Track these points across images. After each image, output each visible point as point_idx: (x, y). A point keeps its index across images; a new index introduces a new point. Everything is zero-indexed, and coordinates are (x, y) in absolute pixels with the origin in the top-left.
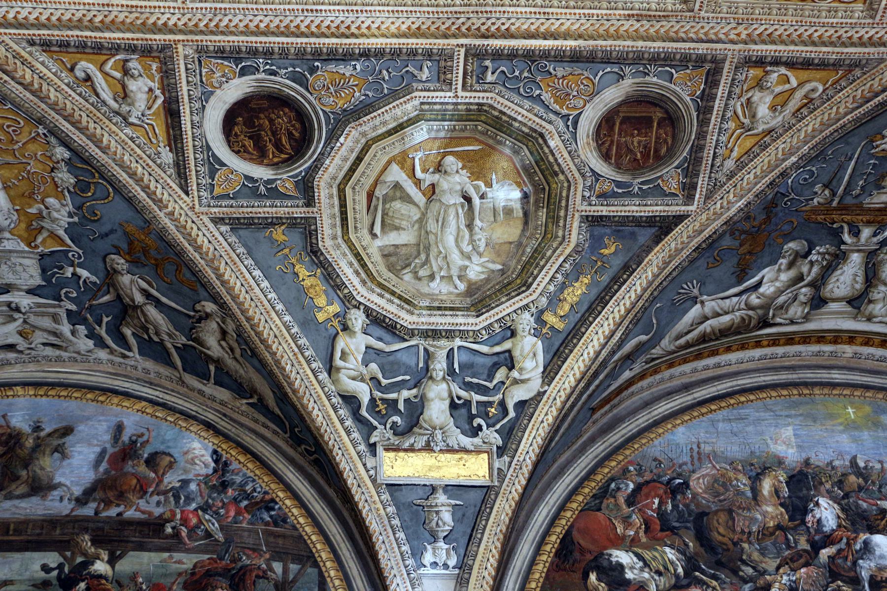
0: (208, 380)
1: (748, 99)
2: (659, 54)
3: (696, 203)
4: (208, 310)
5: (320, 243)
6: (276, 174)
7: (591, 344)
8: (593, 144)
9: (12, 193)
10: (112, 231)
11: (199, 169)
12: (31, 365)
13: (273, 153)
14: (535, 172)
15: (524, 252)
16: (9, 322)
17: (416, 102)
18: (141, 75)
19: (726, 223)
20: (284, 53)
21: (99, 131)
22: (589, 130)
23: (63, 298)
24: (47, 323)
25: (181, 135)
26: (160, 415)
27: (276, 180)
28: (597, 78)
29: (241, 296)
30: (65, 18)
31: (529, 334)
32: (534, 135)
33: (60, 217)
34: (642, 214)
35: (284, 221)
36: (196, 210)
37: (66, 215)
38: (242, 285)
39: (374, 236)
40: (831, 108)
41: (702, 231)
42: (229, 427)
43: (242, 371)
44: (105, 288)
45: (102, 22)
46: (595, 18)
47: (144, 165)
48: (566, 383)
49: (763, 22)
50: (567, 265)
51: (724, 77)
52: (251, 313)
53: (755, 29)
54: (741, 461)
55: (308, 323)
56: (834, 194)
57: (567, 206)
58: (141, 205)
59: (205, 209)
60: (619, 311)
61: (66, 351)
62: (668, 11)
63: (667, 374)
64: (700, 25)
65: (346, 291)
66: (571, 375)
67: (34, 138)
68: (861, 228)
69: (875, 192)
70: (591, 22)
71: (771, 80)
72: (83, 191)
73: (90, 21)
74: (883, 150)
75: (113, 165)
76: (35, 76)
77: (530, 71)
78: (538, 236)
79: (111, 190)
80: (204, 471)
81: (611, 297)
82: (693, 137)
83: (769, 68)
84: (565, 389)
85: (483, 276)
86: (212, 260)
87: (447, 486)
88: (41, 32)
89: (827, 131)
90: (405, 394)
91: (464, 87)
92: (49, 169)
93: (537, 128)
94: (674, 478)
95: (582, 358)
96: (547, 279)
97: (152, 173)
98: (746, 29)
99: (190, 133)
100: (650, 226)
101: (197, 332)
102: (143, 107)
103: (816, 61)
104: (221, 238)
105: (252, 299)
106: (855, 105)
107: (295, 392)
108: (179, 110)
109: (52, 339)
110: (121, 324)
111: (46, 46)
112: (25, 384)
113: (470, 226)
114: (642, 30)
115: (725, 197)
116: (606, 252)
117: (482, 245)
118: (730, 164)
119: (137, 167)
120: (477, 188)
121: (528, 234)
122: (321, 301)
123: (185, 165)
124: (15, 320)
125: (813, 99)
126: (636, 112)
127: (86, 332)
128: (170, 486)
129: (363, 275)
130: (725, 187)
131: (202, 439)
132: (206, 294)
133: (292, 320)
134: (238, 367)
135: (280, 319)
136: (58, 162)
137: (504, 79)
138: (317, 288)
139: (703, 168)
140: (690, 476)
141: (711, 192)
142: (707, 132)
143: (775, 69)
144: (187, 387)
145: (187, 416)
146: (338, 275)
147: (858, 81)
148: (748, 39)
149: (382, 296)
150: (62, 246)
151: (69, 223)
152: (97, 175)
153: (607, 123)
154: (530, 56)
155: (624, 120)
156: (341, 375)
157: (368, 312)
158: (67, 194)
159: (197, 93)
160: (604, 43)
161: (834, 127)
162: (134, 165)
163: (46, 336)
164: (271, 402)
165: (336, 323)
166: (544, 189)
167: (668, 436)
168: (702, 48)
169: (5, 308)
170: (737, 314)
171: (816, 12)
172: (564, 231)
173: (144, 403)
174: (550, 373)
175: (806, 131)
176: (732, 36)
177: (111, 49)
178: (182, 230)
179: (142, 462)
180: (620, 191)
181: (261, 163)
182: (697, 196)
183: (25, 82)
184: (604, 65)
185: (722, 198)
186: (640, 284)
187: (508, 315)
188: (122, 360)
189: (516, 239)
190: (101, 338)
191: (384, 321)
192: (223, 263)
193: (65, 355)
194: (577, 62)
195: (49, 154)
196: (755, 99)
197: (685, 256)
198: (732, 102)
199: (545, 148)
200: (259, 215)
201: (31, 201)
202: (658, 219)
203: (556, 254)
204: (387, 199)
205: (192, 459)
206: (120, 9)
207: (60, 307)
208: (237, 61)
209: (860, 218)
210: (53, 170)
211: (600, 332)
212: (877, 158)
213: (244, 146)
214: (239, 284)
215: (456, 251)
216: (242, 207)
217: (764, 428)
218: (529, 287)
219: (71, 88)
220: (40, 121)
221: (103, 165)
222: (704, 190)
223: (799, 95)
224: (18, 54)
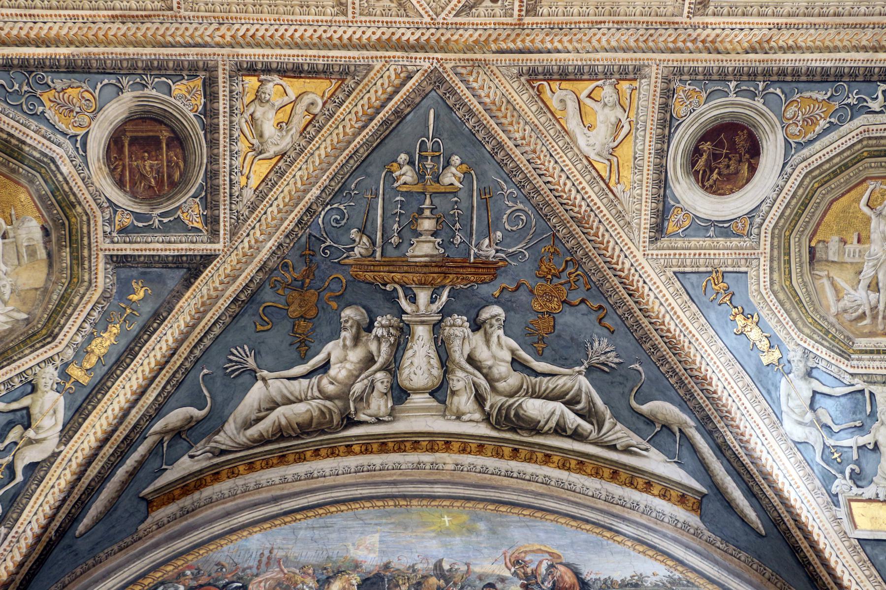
1: (251, 115)
2: (151, 61)
3: (221, 240)
7: (117, 399)
8: (105, 170)
14: (52, 204)
15: (50, 299)
19: (260, 269)
22: (99, 152)
28: (97, 91)
31: (52, 389)
32: (45, 160)
34: (168, 253)
40: (337, 127)
41: (236, 278)
46: (81, 20)
48: (86, 442)
49: (243, 21)
50: (95, 314)
51: (221, 89)
53: (238, 30)
54: (313, 566)
56: (374, 243)
57: (90, 244)
60: (149, 364)
62: (149, 10)
63: (252, 479)
64: (184, 26)
66: (91, 434)
68: (415, 291)
69: (414, 240)
70: (78, 25)
71: (268, 91)
74: (405, 183)
77: (28, 84)
78: (63, 281)
81: (141, 348)
82: (205, 161)
83: (262, 77)
84: (83, 449)
85: (7, 327)
89: (341, 158)
93: (47, 151)
94: (234, 582)
95: (105, 415)
96: (75, 329)
98: (228, 30)
100: (177, 267)
103: (306, 67)
106: (360, 124)
114: (129, 33)
115: (252, 233)
116: (134, 297)
118: (249, 195)
121: (53, 279)
125: (315, 115)
126: (142, 132)
130: (249, 222)
139: (222, 198)
140: (251, 580)
141: (235, 227)
142: (218, 155)
143: (269, 77)
147: (354, 94)
148: (233, 41)
153: (115, 142)
154: (25, 66)
155: (134, 141)
160: (96, 50)
161: (347, 152)
166: (63, 224)
167: (240, 542)
168: (192, 54)
170: (314, 403)
171: (289, 7)
172: (90, 274)
174: (68, 432)
175: (319, 155)
176: (218, 39)
180: (140, 225)
182: (222, 232)
184: (102, 76)
185: (248, 235)
186: (172, 334)
187: (31, 368)
189: (42, 285)
194: (74, 72)
196: (258, 115)
197: (223, 308)
198: (236, 119)
199: (59, 176)
202: (184, 259)
203: (84, 301)
209: (410, 276)
211: (127, 387)
212: (403, 194)
217: (348, 535)
218: (55, 338)
222: (228, 224)
223: (300, 108)
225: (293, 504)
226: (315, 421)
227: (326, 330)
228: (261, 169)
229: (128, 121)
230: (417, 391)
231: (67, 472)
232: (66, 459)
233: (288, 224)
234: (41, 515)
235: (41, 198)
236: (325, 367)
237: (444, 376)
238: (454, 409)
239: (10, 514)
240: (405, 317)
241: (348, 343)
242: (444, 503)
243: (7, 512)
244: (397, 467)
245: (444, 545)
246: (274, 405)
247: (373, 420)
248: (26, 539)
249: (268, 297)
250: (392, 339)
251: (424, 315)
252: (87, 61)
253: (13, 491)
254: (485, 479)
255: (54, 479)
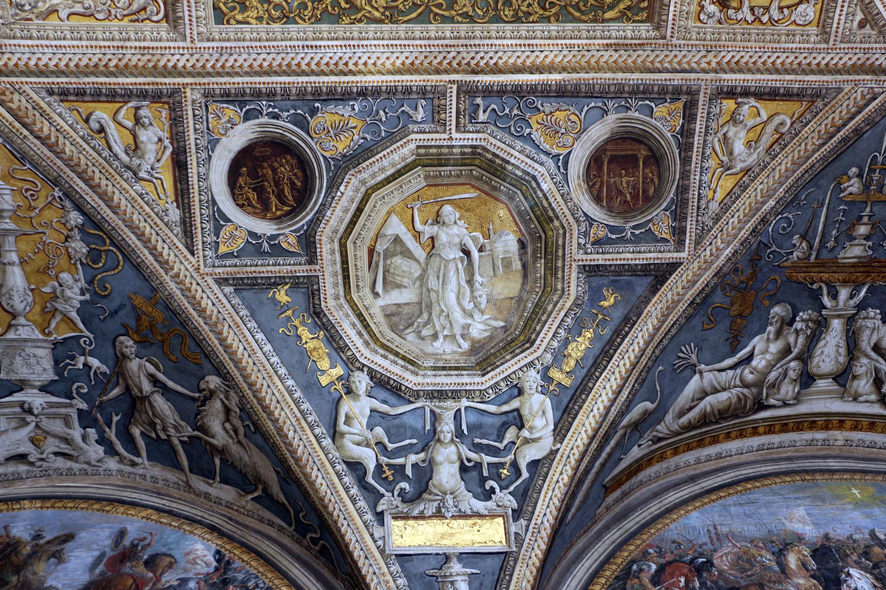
0: (214, 479)
1: (724, 135)
2: (638, 86)
3: (687, 249)
4: (212, 386)
5: (323, 304)
6: (279, 229)
7: (600, 399)
8: (584, 186)
9: (28, 268)
10: (122, 307)
11: (204, 226)
12: (42, 480)
13: (276, 205)
14: (531, 218)
15: (525, 307)
16: (21, 426)
17: (412, 146)
18: (151, 124)
19: (716, 274)
20: (286, 93)
21: (110, 188)
22: (579, 170)
23: (75, 395)
24: (57, 426)
25: (188, 189)
26: (165, 521)
27: (279, 235)
28: (583, 114)
29: (244, 361)
30: (82, 63)
31: (537, 391)
32: (527, 178)
33: (72, 295)
34: (637, 262)
35: (287, 280)
36: (201, 271)
37: (79, 292)
38: (245, 349)
39: (376, 295)
40: (800, 145)
41: (695, 282)
42: (234, 530)
43: (246, 458)
44: (114, 379)
45: (116, 66)
46: (576, 48)
47: (152, 224)
48: (579, 440)
49: (730, 49)
50: (569, 320)
51: (700, 111)
52: (253, 378)
53: (724, 57)
54: (760, 539)
55: (311, 387)
56: (811, 247)
57: (564, 255)
58: (148, 271)
59: (209, 270)
60: (624, 365)
61: (77, 462)
62: (642, 39)
63: (673, 462)
64: (673, 53)
65: (349, 353)
66: (583, 432)
67: (50, 203)
68: (838, 288)
69: (847, 244)
70: (573, 53)
71: (743, 113)
72: (95, 262)
73: (106, 66)
74: (851, 194)
75: (123, 227)
76: (53, 129)
77: (519, 108)
78: (537, 290)
79: (121, 258)
80: (205, 570)
81: (615, 351)
82: (678, 177)
83: (740, 100)
84: (578, 447)
85: (486, 334)
86: (215, 324)
87: (461, 553)
88: (60, 80)
89: (798, 172)
90: (413, 458)
91: (458, 130)
92: (63, 238)
93: (530, 170)
94: (697, 558)
95: (592, 414)
96: (550, 335)
97: (159, 232)
98: (715, 57)
99: (196, 187)
100: (646, 275)
101: (202, 418)
102: (153, 159)
103: (782, 91)
104: (224, 301)
105: (254, 364)
106: (821, 141)
107: (297, 460)
108: (186, 162)
109: (64, 448)
110: (130, 423)
111: (64, 94)
112: (32, 498)
113: (470, 282)
114: (620, 60)
115: (714, 242)
116: (605, 304)
117: (483, 301)
118: (714, 207)
119: (145, 227)
120: (474, 239)
121: (528, 288)
122: (324, 364)
123: (191, 222)
124: (28, 424)
125: (782, 134)
126: (622, 150)
127: (96, 437)
128: (168, 584)
129: (366, 336)
130: (713, 232)
131: (205, 541)
132: (210, 366)
133: (294, 384)
134: (242, 452)
135: (283, 383)
136: (71, 230)
137: (496, 118)
138: (320, 351)
139: (690, 211)
140: (712, 555)
141: (700, 237)
142: (689, 171)
143: (746, 100)
144: (194, 492)
145: (192, 521)
146: (341, 337)
147: (821, 114)
148: (718, 68)
149: (386, 357)
150: (74, 331)
151: (81, 302)
152: (108, 241)
153: (595, 161)
154: (518, 91)
155: (612, 160)
156: (345, 440)
157: (372, 374)
158: (79, 266)
159: (203, 142)
160: (586, 76)
161: (804, 167)
162: (142, 224)
163: (57, 444)
164: (275, 489)
165: (339, 387)
166: (540, 237)
167: (682, 521)
168: (677, 79)
169: (18, 410)
170: (734, 391)
171: (776, 36)
172: (563, 283)
173: (149, 511)
174: (561, 430)
175: (780, 170)
176: (704, 65)
177: (123, 96)
178: (187, 294)
179: (141, 563)
180: (614, 237)
181: (264, 218)
182: (687, 242)
183: (43, 136)
184: (589, 100)
185: (711, 244)
186: (643, 337)
187: (514, 372)
188: (129, 469)
189: (517, 294)
190: (111, 442)
191: (388, 383)
192: (226, 327)
193: (76, 466)
194: (563, 96)
195: (63, 221)
196: (730, 134)
197: (681, 310)
198: (710, 138)
199: (539, 192)
200: (262, 275)
201: (45, 278)
202: (652, 267)
203: (557, 309)
204: (388, 254)
205: (194, 559)
206: (133, 51)
207: (71, 406)
208: (242, 104)
209: (836, 276)
210: (67, 238)
211: (608, 387)
212: (846, 203)
213: (248, 199)
214: (241, 348)
215: (458, 309)
216: (246, 266)
217: (776, 509)
218: (533, 344)
219: (85, 141)
220: (56, 182)
221: (114, 229)
222: (693, 234)
223: (770, 128)
224: (38, 105)
225: (710, 482)
226: (732, 406)
227: (756, 325)
228: (728, 183)
229: (608, 141)
230: (822, 377)
231: (568, 467)
232: (565, 456)
233: (744, 234)
234: (552, 507)
235: (520, 213)
236: (750, 357)
237: (849, 363)
238: (853, 391)
239: (525, 507)
240: (824, 312)
241: (771, 336)
242: (845, 477)
243: (522, 506)
244: (793, 445)
245: (868, 516)
246: (705, 394)
247: (780, 403)
248: (545, 529)
249: (719, 299)
250: (809, 332)
251: (841, 310)
252: (577, 86)
253: (523, 487)
254: (873, 452)
255: (557, 475)
